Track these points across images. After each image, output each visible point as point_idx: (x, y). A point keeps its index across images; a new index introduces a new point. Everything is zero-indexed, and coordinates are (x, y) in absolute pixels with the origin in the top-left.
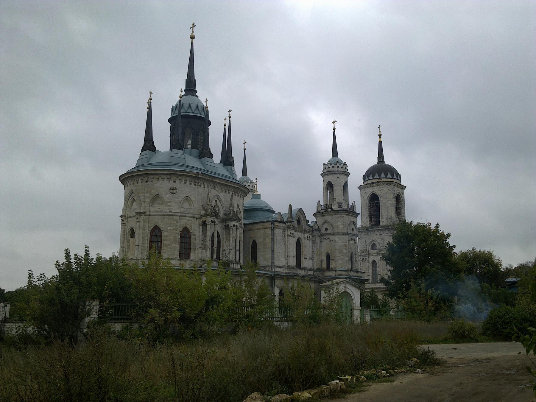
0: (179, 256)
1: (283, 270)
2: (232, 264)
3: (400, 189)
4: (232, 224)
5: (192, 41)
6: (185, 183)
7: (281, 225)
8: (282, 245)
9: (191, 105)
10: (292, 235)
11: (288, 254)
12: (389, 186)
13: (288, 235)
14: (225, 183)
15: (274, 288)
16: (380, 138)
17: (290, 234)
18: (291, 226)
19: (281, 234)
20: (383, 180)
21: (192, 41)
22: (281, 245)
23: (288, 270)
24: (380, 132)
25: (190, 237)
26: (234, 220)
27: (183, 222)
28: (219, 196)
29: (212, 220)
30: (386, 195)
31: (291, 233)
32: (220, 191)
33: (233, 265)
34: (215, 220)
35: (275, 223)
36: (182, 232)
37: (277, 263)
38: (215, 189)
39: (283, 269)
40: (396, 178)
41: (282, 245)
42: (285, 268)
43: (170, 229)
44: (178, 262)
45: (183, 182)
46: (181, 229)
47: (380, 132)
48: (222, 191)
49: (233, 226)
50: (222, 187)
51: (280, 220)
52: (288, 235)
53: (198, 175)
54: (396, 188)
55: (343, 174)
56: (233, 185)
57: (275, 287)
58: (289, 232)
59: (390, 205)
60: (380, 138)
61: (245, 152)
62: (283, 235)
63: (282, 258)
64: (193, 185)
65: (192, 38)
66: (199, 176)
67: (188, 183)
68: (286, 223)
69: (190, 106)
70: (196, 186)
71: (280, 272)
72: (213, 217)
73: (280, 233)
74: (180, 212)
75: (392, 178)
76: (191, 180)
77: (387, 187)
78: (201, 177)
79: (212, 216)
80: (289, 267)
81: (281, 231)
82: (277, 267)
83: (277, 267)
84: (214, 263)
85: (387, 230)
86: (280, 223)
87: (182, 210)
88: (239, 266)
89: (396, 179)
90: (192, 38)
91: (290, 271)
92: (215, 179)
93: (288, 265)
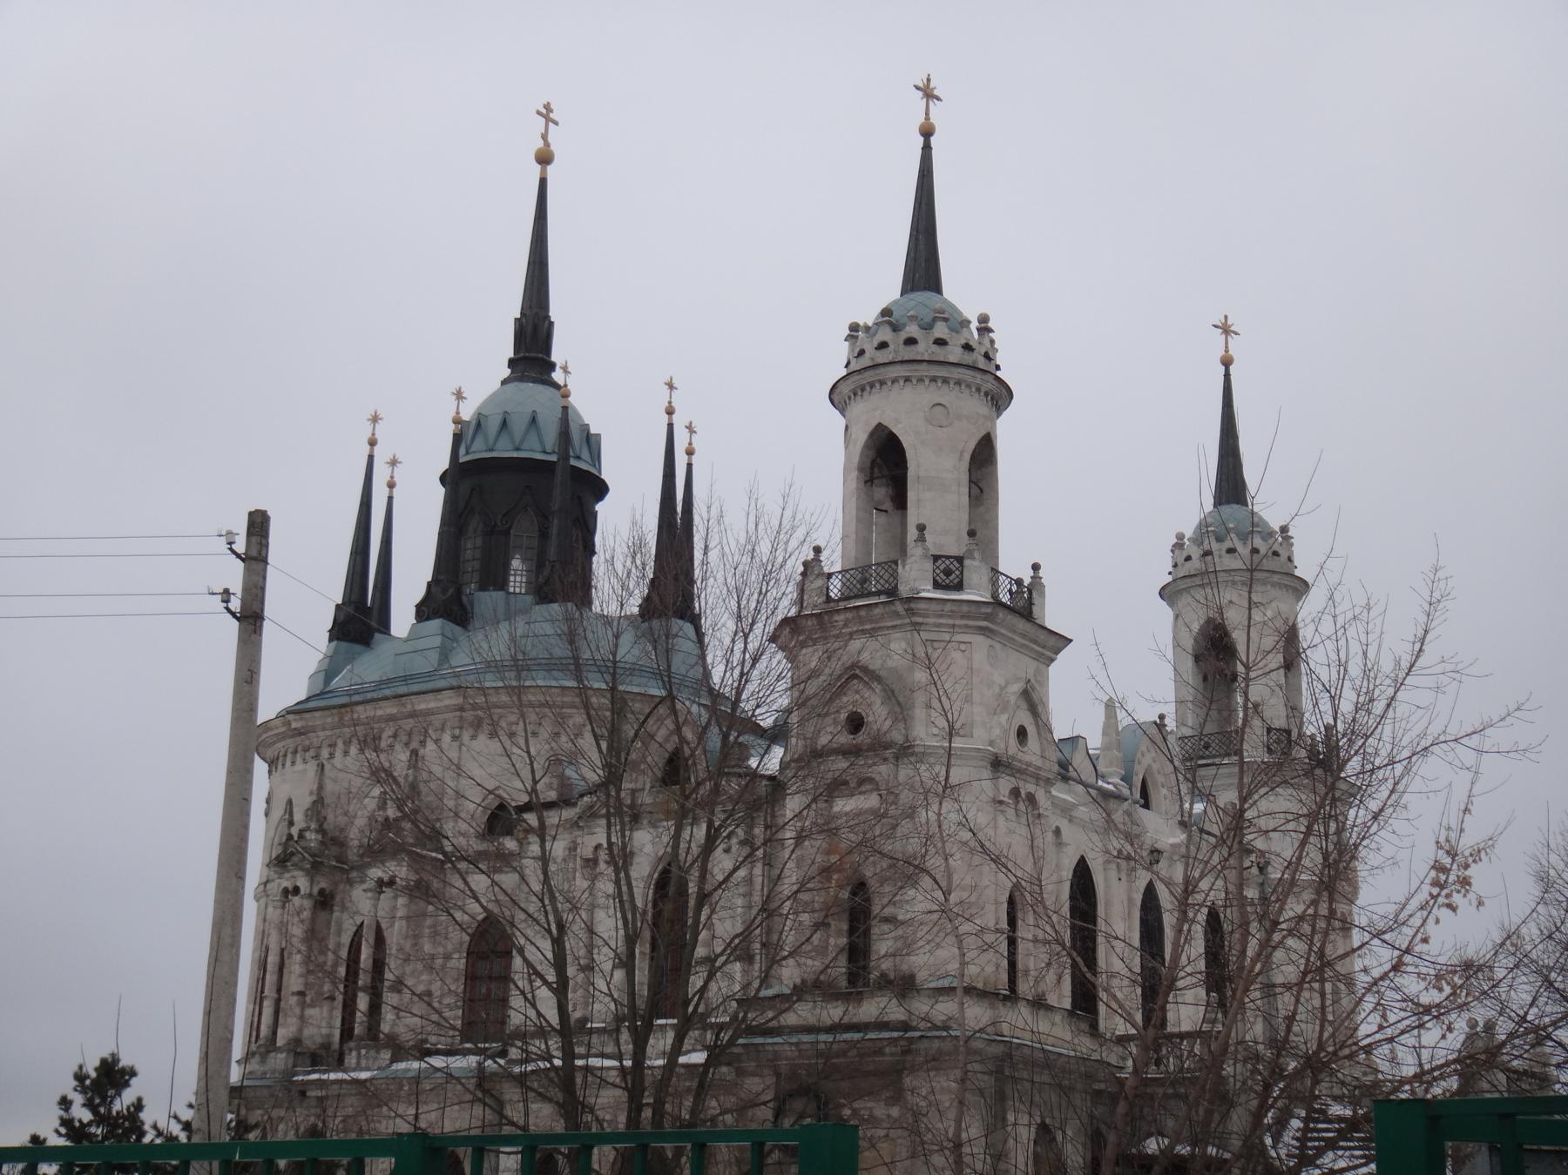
5: (544, 171)
6: (283, 765)
9: (540, 418)
21: (544, 171)
34: (298, 884)
61: (1227, 376)
64: (299, 766)
65: (544, 159)
66: (294, 725)
67: (288, 763)
69: (534, 420)
70: (308, 766)
72: (289, 875)
79: (288, 871)
84: (275, 1058)
90: (544, 159)
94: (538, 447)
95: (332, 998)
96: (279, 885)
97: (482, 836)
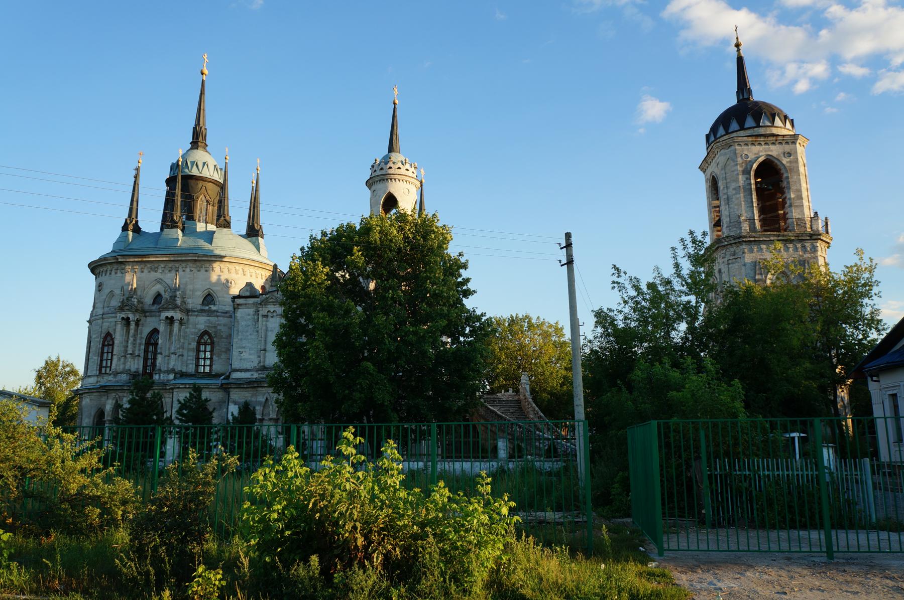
0: (98, 372)
1: (252, 375)
2: (157, 375)
3: (772, 147)
4: (164, 315)
6: (110, 274)
7: (251, 301)
8: (250, 335)
10: (275, 314)
11: (263, 348)
12: (729, 150)
13: (266, 316)
14: (167, 259)
15: (228, 405)
16: (738, 50)
17: (266, 314)
18: (271, 300)
19: (249, 317)
20: (722, 139)
22: (248, 334)
23: (259, 374)
24: (737, 38)
25: (113, 345)
26: (167, 309)
27: (106, 325)
28: (162, 280)
29: (123, 316)
30: (723, 172)
31: (269, 311)
32: (167, 271)
33: (160, 376)
35: (236, 300)
36: (105, 339)
37: (236, 365)
38: (156, 271)
39: (250, 373)
40: (770, 125)
41: (250, 335)
42: (257, 371)
43: (94, 338)
44: (96, 378)
45: (108, 274)
46: (103, 335)
47: (737, 38)
48: (170, 271)
49: (164, 318)
50: (170, 265)
51: (248, 294)
52: (266, 316)
53: (117, 259)
54: (756, 149)
55: (380, 181)
56: (183, 259)
57: (230, 404)
58: (264, 311)
59: (734, 192)
60: (738, 50)
62: (256, 317)
63: (250, 354)
64: (119, 274)
66: (120, 260)
67: (113, 273)
68: (260, 297)
71: (242, 378)
73: (249, 315)
74: (103, 314)
75: (742, 128)
76: (115, 267)
77: (725, 154)
78: (122, 260)
80: (264, 368)
81: (251, 311)
82: (236, 370)
83: (236, 370)
85: (723, 250)
86: (248, 299)
87: (106, 310)
88: (172, 376)
89: (754, 128)
91: (262, 376)
92: (149, 258)
93: (262, 364)
94: (208, 174)
95: (139, 356)
96: (120, 316)
97: (203, 304)
